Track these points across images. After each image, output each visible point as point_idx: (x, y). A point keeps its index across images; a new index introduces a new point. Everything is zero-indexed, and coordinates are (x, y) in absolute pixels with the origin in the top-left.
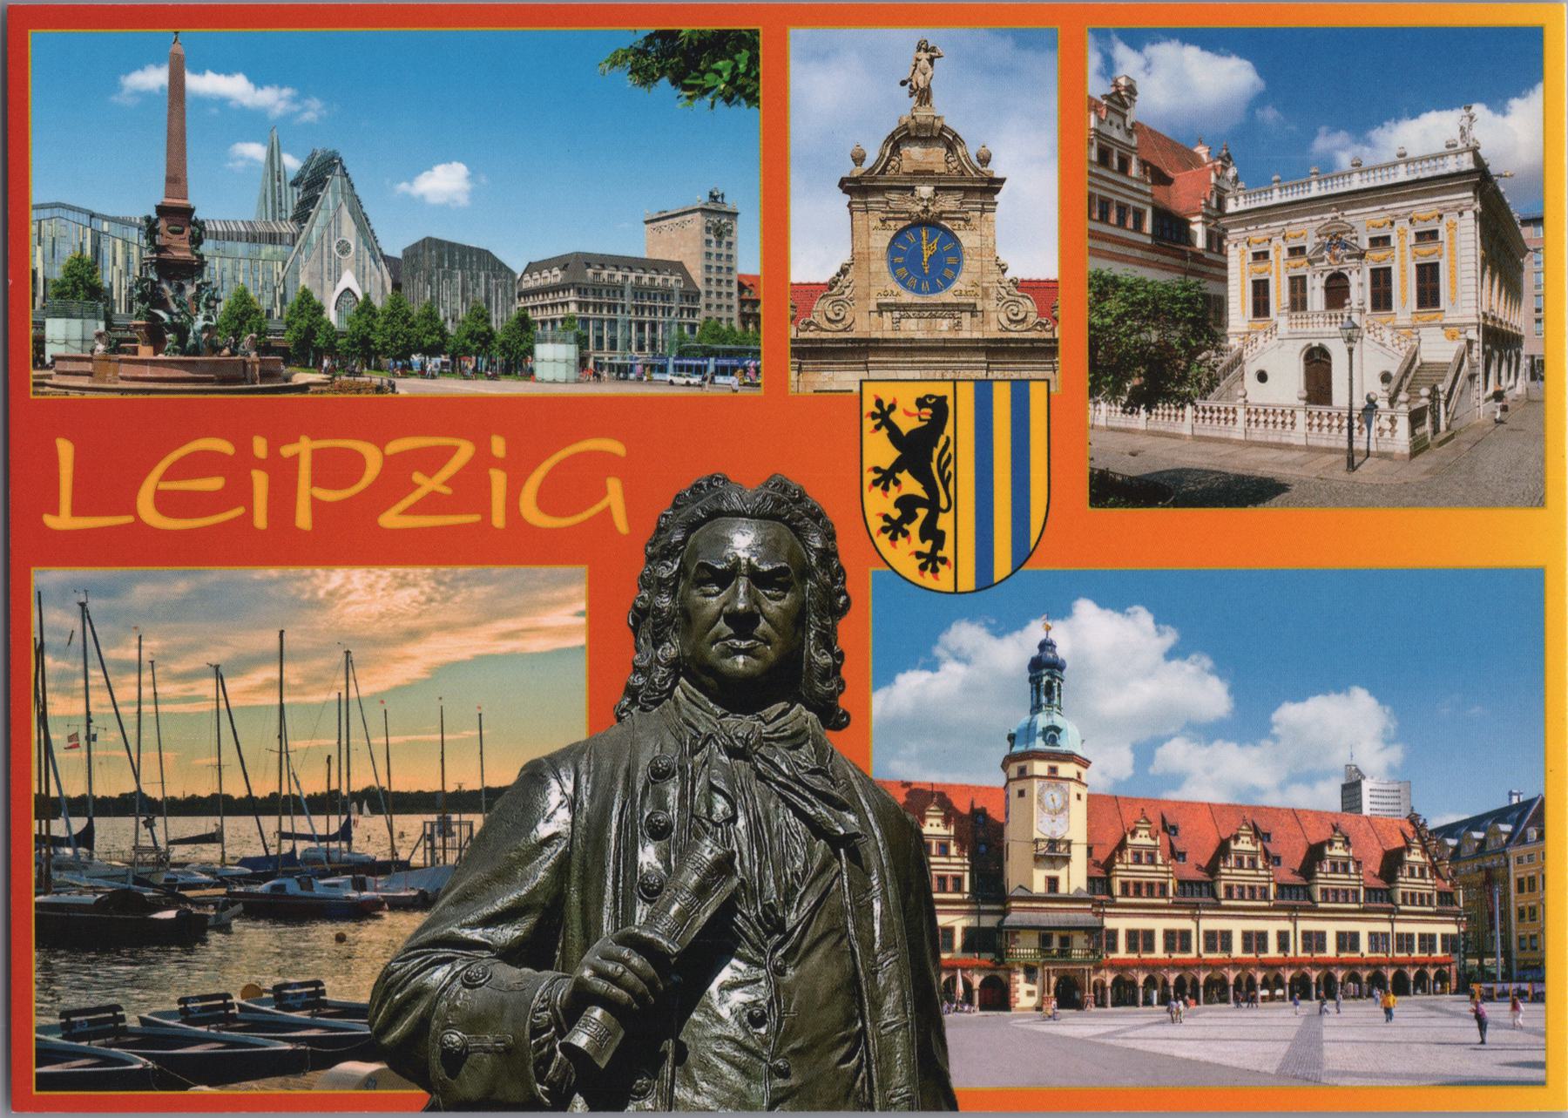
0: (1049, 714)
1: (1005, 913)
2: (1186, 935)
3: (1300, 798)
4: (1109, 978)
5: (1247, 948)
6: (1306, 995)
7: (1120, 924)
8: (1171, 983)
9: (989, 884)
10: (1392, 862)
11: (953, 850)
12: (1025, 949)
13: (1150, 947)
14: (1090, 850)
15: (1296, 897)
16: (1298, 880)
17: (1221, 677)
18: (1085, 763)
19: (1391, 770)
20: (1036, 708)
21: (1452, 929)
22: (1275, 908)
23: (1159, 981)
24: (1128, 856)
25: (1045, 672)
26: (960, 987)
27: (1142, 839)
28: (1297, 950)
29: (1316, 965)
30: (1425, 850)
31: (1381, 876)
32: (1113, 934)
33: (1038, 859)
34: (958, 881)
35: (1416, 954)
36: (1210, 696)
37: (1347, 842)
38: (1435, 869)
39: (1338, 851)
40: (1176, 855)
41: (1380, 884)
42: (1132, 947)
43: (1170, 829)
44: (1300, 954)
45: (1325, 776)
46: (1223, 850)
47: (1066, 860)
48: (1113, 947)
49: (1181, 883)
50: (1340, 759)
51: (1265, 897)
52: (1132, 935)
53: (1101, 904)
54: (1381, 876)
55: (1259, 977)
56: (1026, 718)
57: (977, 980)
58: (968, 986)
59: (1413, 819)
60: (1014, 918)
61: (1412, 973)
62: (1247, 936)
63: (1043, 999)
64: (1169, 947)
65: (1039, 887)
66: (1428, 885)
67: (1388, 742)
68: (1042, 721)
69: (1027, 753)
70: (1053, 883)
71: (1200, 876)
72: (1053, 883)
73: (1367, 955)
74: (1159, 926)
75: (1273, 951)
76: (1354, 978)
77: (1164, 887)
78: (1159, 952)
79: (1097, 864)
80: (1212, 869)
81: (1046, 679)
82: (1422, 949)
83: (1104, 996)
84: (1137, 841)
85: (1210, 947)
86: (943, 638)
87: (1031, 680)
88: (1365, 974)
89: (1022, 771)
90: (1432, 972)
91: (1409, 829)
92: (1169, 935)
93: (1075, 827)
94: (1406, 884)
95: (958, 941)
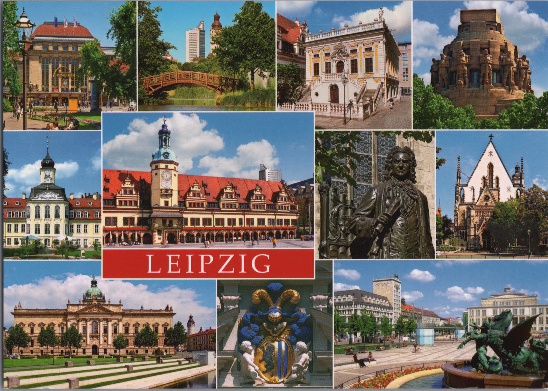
0: (165, 148)
1: (151, 213)
2: (210, 220)
3: (246, 175)
4: (185, 234)
5: (229, 223)
6: (248, 239)
7: (189, 216)
8: (205, 235)
9: (146, 203)
10: (276, 196)
11: (134, 193)
12: (157, 225)
13: (198, 224)
14: (179, 192)
15: (245, 208)
16: (245, 202)
17: (221, 136)
18: (177, 164)
19: (275, 166)
20: (161, 146)
21: (295, 218)
22: (238, 211)
23: (201, 235)
24: (191, 194)
25: (164, 135)
26: (136, 236)
27: (196, 189)
28: (245, 224)
29: (251, 229)
30: (286, 192)
31: (272, 201)
32: (186, 219)
33: (162, 195)
34: (136, 203)
35: (283, 226)
36: (216, 142)
37: (261, 190)
38: (289, 198)
39: (258, 192)
40: (206, 194)
41: (271, 203)
42: (192, 223)
43: (205, 186)
44: (246, 226)
45: (254, 168)
46: (222, 192)
47: (171, 195)
48: (186, 224)
49: (208, 203)
50: (259, 162)
51: (235, 207)
52: (192, 220)
53: (182, 210)
54: (272, 201)
55: (233, 233)
56: (158, 150)
57: (142, 234)
58: (139, 236)
59: (282, 182)
60: (154, 214)
61: (282, 232)
62: (229, 220)
63: (163, 241)
64: (204, 224)
65: (162, 204)
66: (287, 203)
67: (274, 157)
68: (163, 150)
69: (159, 161)
70: (166, 203)
71: (214, 201)
72: (166, 203)
73: (267, 226)
74: (201, 217)
75: (237, 225)
76: (263, 233)
77: (203, 204)
78: (201, 225)
79: (181, 197)
80: (218, 198)
81: (164, 137)
82: (285, 224)
83: (183, 240)
84: (194, 189)
85: (217, 223)
86: (131, 124)
87: (159, 137)
88: (267, 232)
89: (157, 167)
90: (288, 232)
91: (281, 185)
92: (204, 220)
93: (174, 185)
94: (280, 203)
95: (136, 222)
